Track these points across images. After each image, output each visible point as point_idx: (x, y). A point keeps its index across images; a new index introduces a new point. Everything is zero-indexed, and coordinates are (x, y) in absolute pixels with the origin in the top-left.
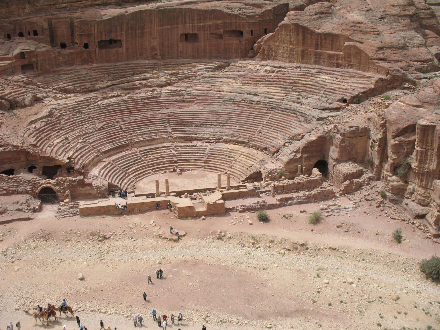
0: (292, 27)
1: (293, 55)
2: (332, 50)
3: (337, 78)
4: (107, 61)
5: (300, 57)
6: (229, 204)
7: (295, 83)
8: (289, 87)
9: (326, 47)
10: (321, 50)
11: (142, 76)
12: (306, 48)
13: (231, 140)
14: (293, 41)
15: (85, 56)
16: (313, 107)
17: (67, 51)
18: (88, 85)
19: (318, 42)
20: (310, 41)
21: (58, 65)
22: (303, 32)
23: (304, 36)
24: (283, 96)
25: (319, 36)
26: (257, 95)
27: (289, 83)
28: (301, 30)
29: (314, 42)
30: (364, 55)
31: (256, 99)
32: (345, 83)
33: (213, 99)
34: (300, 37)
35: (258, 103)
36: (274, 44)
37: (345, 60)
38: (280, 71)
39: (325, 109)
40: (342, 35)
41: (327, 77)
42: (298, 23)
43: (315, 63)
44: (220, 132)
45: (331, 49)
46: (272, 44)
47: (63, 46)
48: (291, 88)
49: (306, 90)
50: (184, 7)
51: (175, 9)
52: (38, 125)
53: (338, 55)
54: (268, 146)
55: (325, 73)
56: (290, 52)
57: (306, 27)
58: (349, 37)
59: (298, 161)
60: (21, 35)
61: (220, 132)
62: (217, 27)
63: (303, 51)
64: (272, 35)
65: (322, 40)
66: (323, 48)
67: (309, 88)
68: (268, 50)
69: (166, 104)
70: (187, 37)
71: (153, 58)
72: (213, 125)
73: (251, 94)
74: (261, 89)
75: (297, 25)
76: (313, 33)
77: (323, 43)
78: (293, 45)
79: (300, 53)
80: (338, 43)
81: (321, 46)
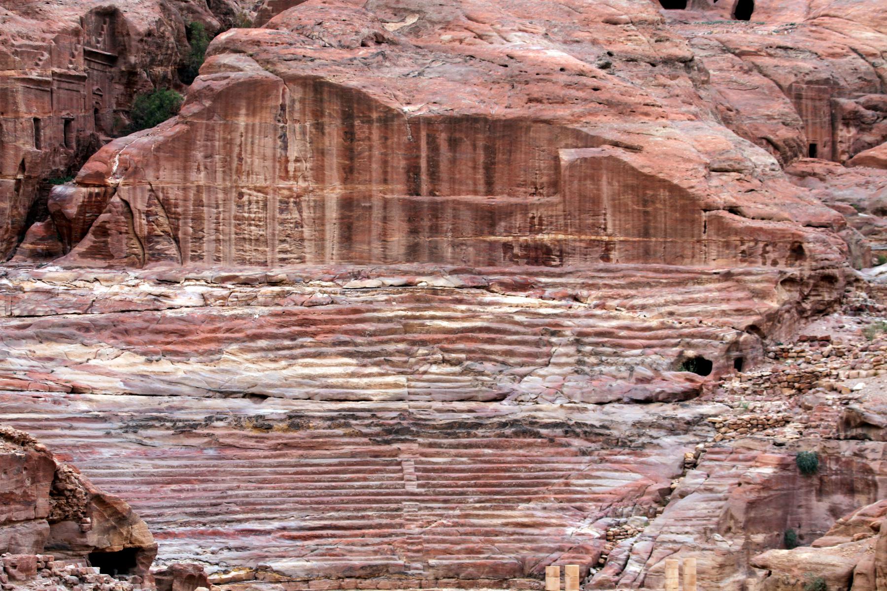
0: (293, 94)
1: (299, 224)
2: (490, 192)
3: (576, 299)
5: (332, 232)
7: (407, 329)
8: (391, 347)
9: (461, 183)
10: (432, 193)
12: (361, 187)
13: (310, 571)
14: (297, 160)
16: (595, 398)
19: (418, 157)
20: (376, 153)
22: (347, 117)
23: (349, 135)
24: (396, 385)
25: (423, 134)
26: (263, 397)
27: (373, 334)
28: (332, 108)
29: (400, 163)
30: (663, 194)
31: (266, 409)
32: (632, 308)
33: (75, 424)
34: (333, 140)
35: (295, 421)
36: (185, 179)
37: (566, 225)
38: (283, 295)
39: (647, 401)
40: (537, 121)
41: (520, 299)
42: (321, 73)
43: (413, 252)
44: (237, 549)
45: (481, 188)
46: (167, 179)
48: (407, 353)
49: (484, 351)
53: (525, 209)
54: (530, 556)
55: (501, 284)
56: (282, 211)
57: (359, 92)
58: (576, 126)
59: (739, 566)
61: (237, 549)
63: (347, 204)
64: (175, 138)
65: (434, 147)
66: (444, 187)
67: (492, 341)
68: (148, 214)
72: (175, 523)
73: (226, 394)
75: (316, 87)
76: (389, 117)
77: (444, 165)
78: (295, 178)
79: (332, 213)
80: (520, 156)
81: (434, 175)
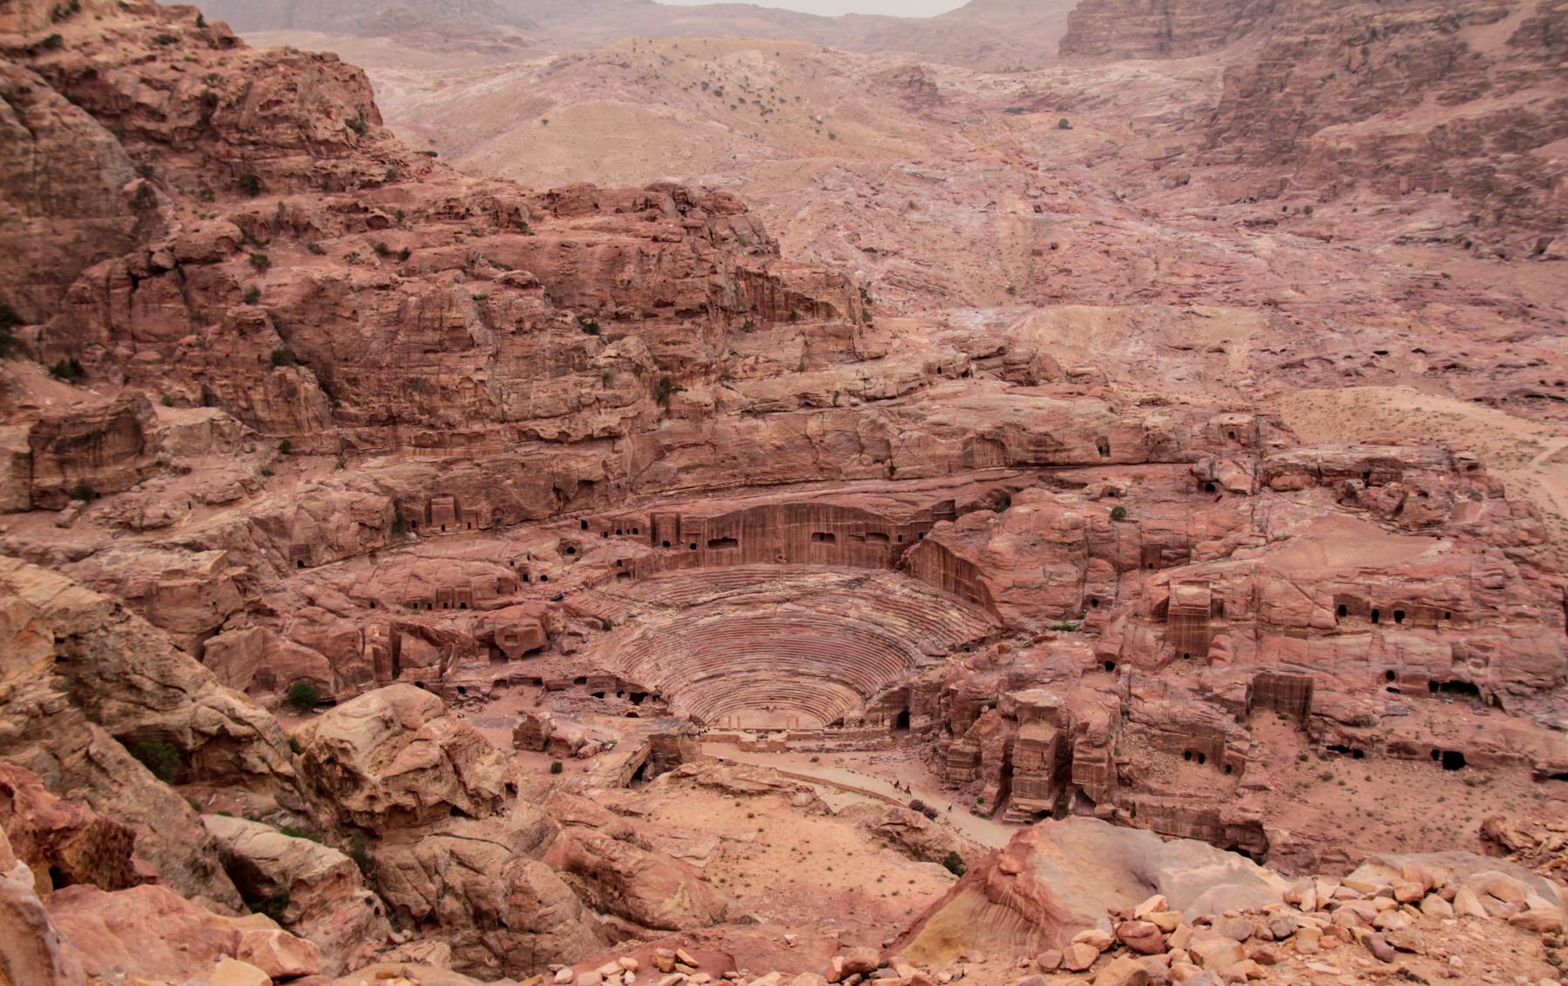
4: (718, 564)
6: (791, 744)
11: (756, 588)
15: (691, 559)
17: (671, 552)
18: (690, 598)
21: (658, 570)
47: (666, 544)
50: (816, 501)
51: (804, 505)
52: (629, 649)
60: (619, 532)
62: (858, 528)
69: (775, 628)
70: (822, 537)
71: (776, 562)
74: (890, 618)
